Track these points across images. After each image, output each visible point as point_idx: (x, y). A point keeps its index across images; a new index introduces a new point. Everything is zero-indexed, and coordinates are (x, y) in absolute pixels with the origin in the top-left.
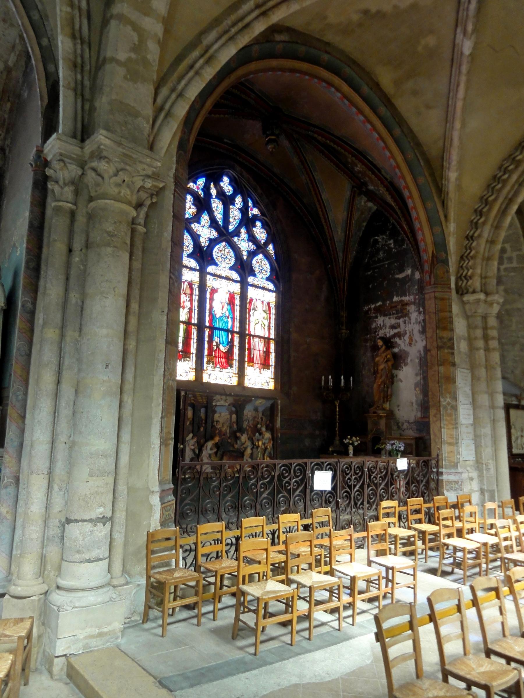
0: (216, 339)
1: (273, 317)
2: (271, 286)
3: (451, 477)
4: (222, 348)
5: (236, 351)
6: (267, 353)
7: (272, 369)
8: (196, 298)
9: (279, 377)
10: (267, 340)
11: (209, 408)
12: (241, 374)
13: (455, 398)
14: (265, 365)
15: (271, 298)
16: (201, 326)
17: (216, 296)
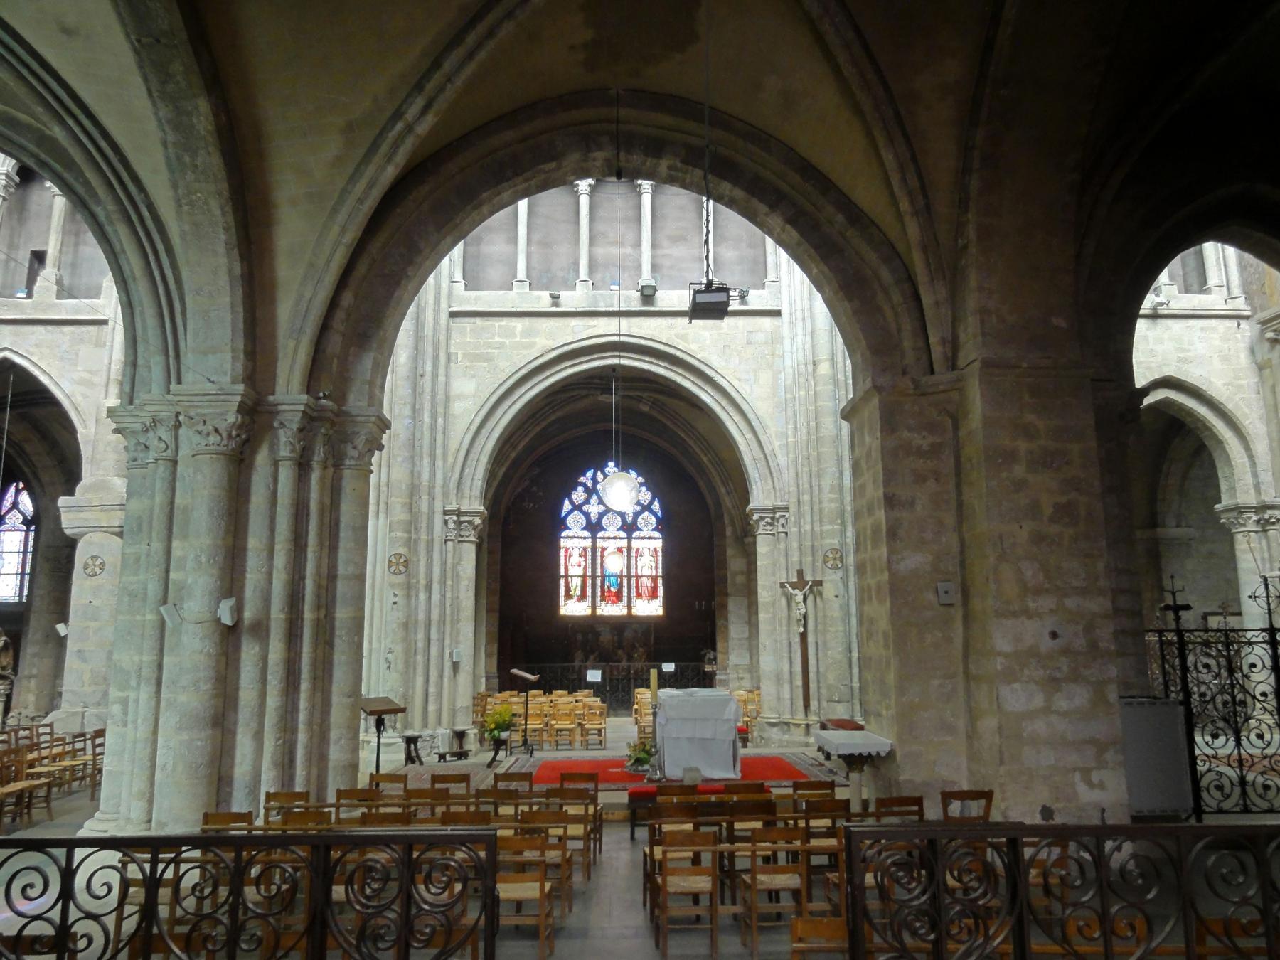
0: (607, 584)
1: (660, 558)
2: (657, 534)
3: (723, 677)
4: (612, 589)
5: (625, 590)
6: (655, 588)
7: (661, 599)
8: (589, 557)
9: (667, 605)
10: (654, 579)
11: (597, 634)
12: (629, 607)
13: (727, 620)
14: (654, 595)
15: (659, 544)
16: (594, 577)
17: (606, 553)
